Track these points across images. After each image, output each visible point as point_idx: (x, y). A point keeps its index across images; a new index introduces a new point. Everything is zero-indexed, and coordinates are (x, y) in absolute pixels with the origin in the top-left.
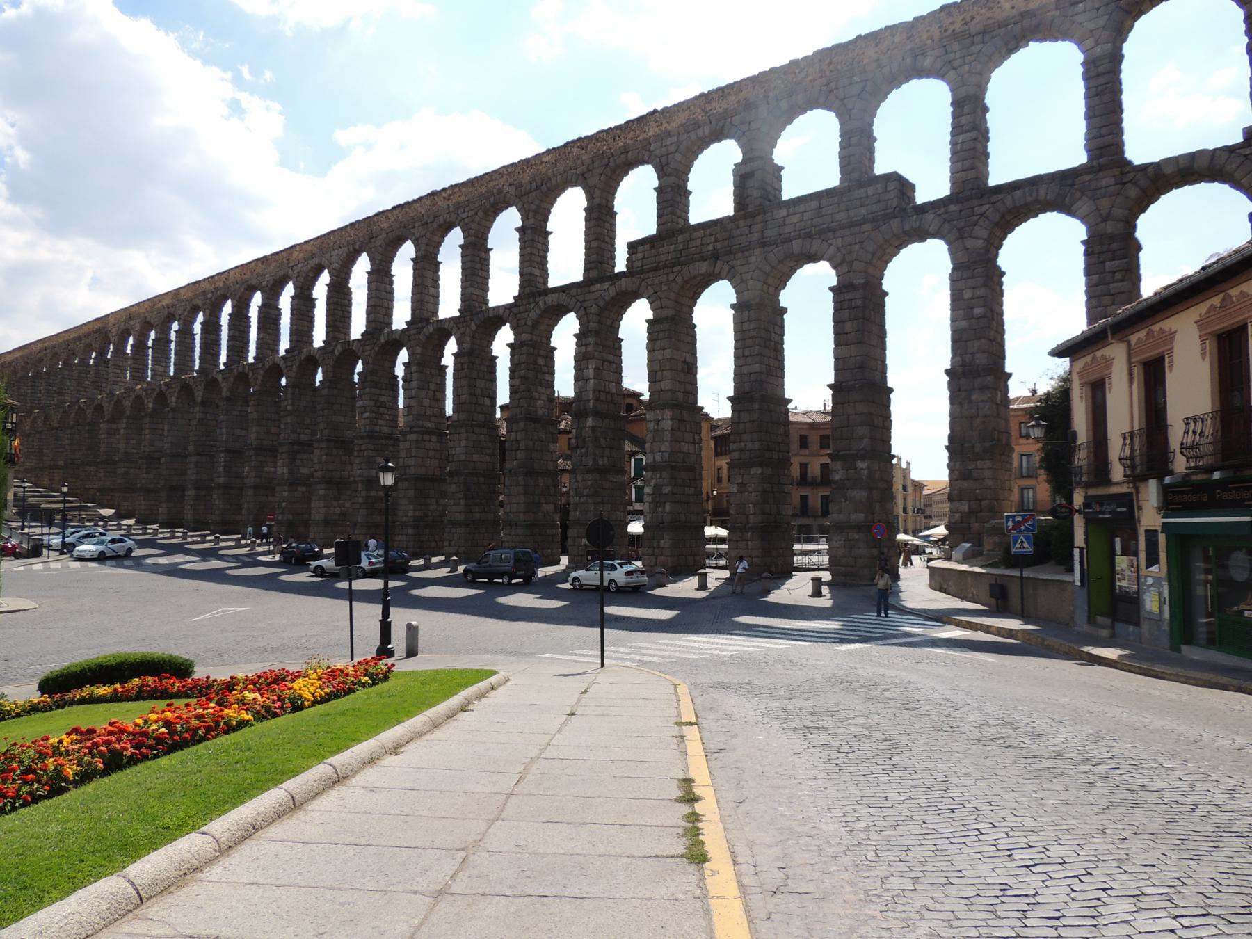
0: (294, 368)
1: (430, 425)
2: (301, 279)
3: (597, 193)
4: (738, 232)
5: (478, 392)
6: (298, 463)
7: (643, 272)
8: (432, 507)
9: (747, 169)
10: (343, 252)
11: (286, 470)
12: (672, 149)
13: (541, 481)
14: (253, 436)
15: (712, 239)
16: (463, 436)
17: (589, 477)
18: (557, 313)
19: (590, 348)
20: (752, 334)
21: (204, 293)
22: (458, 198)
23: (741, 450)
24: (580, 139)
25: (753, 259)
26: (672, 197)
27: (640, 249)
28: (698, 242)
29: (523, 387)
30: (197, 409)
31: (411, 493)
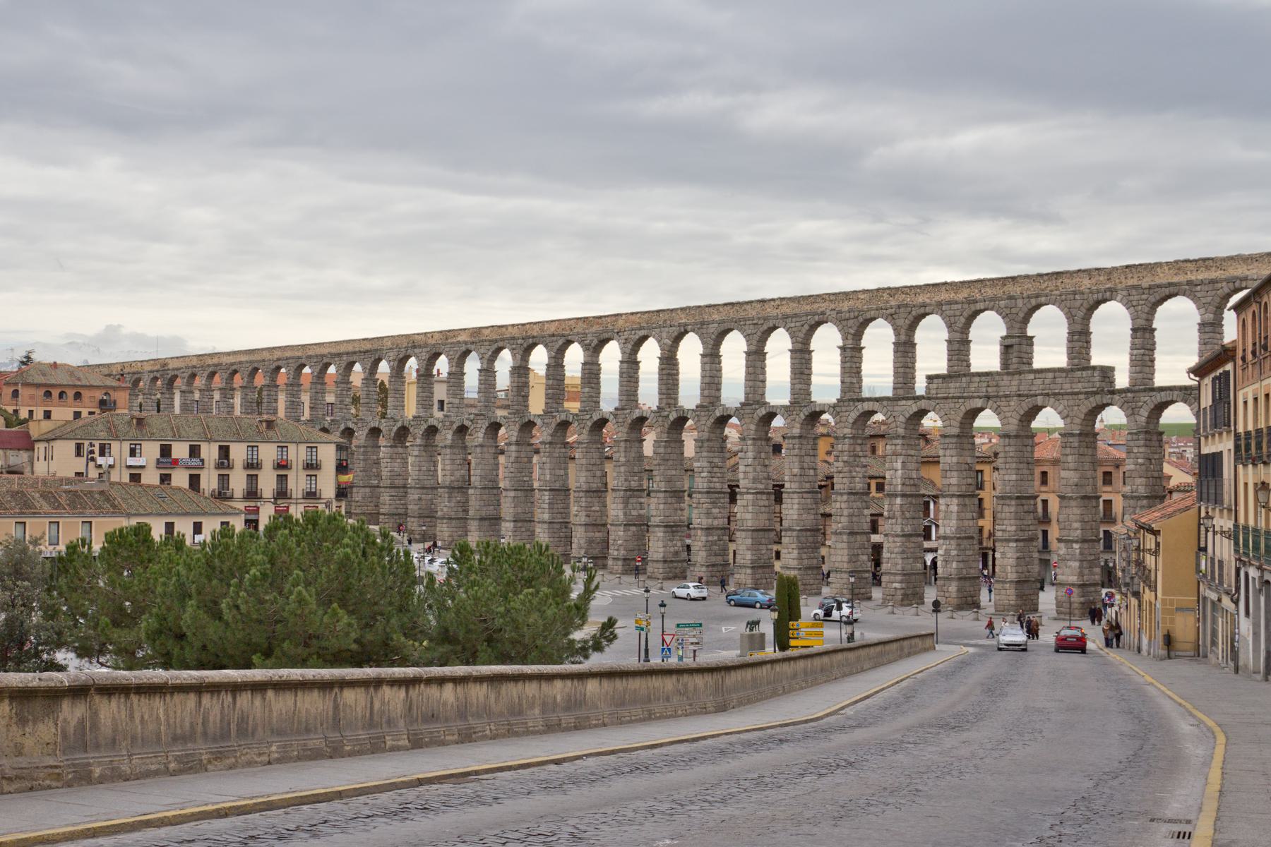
1: (762, 486)
3: (903, 331)
5: (806, 466)
6: (630, 506)
9: (1009, 342)
10: (675, 331)
11: (621, 514)
12: (958, 313)
16: (796, 501)
21: (513, 338)
22: (786, 309)
24: (889, 288)
25: (1012, 403)
26: (959, 347)
29: (846, 469)
31: (749, 541)
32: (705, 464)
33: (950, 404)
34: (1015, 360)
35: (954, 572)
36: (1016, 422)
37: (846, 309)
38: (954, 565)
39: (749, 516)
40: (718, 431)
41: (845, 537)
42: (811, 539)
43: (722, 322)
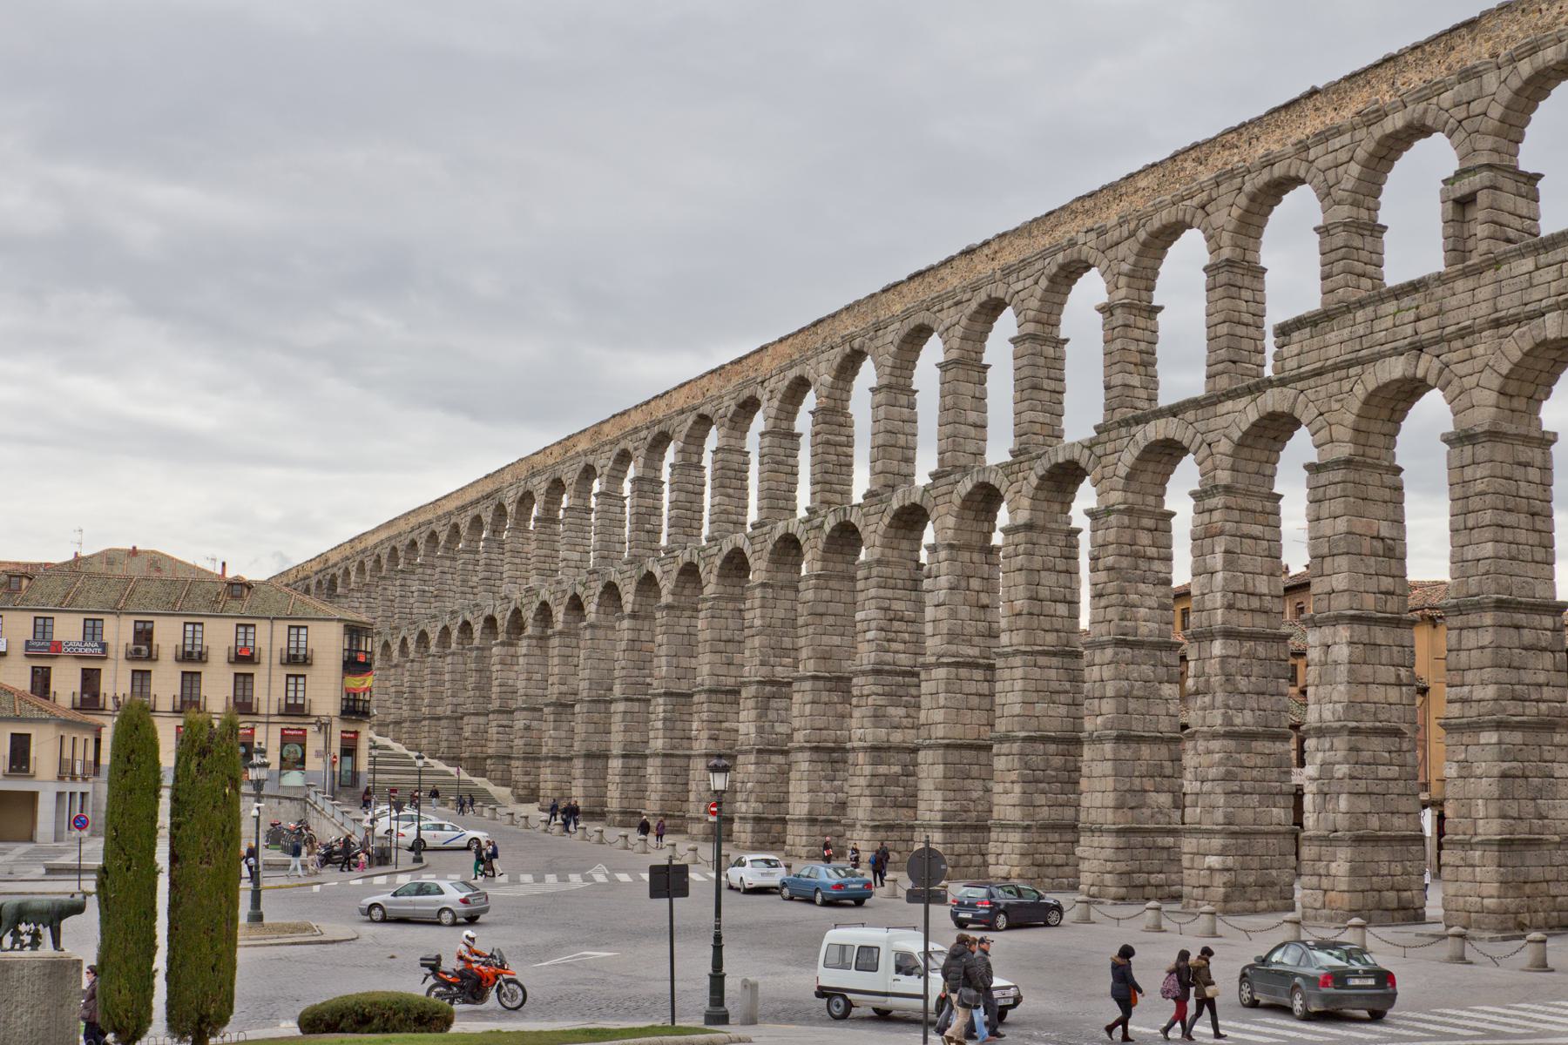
0: (766, 555)
2: (775, 403)
3: (1226, 238)
4: (1453, 302)
5: (1044, 592)
6: (772, 715)
7: (1300, 378)
8: (975, 795)
9: (1464, 187)
13: (1145, 750)
14: (706, 669)
15: (1411, 315)
16: (1019, 673)
17: (1216, 745)
18: (1167, 453)
19: (1217, 515)
20: (1480, 487)
23: (1463, 701)
25: (1480, 350)
27: (1296, 336)
28: (1389, 322)
30: (626, 623)
31: (939, 770)
32: (873, 613)
33: (1329, 384)
34: (1481, 230)
35: (1342, 821)
36: (1490, 397)
37: (1114, 220)
38: (1343, 803)
39: (939, 715)
40: (905, 545)
41: (1108, 748)
42: (1057, 761)
43: (907, 315)
